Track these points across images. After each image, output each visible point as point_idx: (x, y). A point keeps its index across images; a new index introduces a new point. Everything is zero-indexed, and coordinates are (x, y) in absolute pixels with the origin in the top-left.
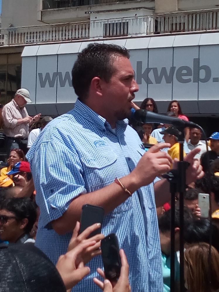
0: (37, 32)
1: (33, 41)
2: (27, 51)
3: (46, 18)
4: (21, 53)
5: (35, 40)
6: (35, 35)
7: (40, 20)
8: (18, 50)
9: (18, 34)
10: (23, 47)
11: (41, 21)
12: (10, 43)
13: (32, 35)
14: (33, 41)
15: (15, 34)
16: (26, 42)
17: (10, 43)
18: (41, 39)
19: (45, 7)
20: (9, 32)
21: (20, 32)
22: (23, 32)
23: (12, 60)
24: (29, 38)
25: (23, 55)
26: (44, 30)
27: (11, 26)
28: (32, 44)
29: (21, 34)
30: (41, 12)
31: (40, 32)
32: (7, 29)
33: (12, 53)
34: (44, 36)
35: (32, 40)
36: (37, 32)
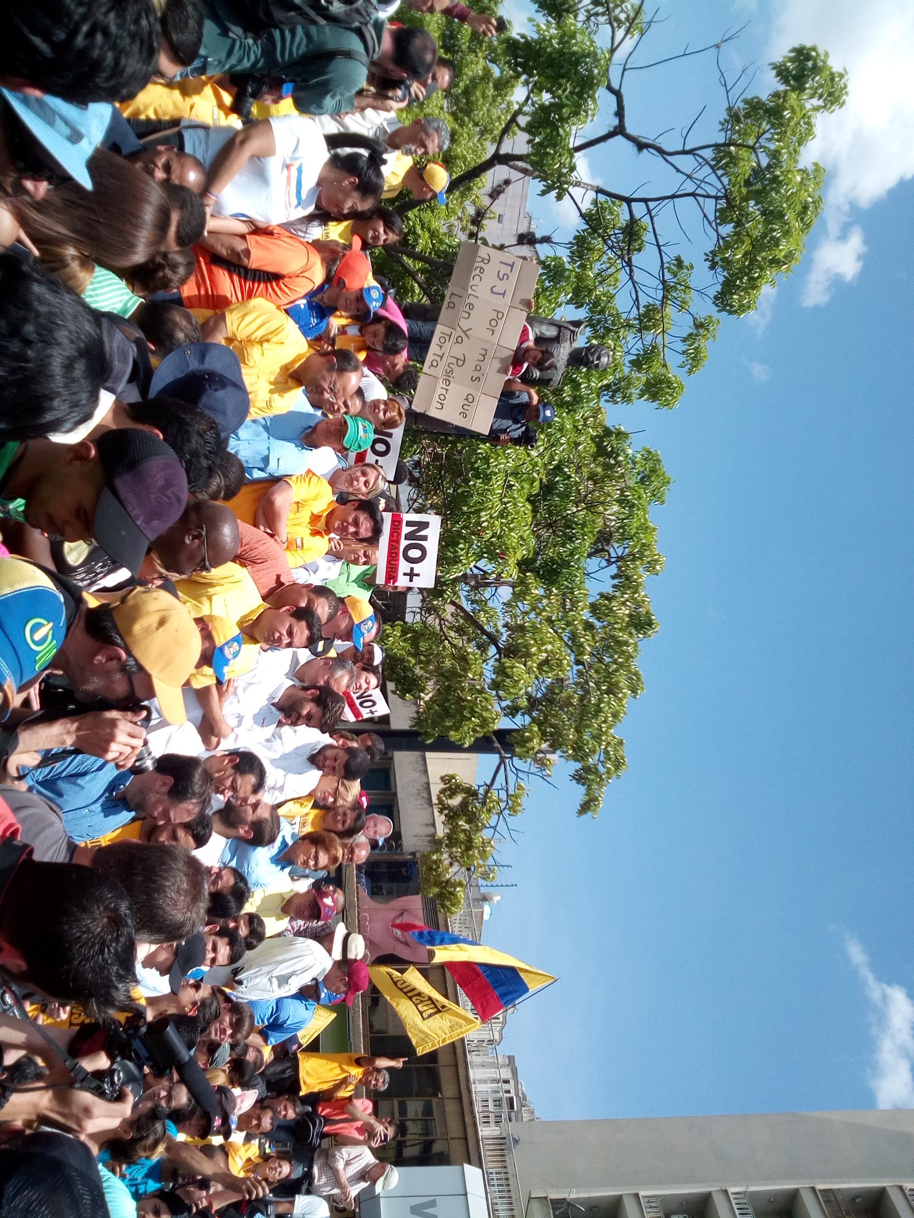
0: (509, 1191)
1: (494, 1185)
2: (473, 1174)
3: (535, 1205)
4: (470, 1163)
5: (496, 1188)
6: (505, 1188)
7: (532, 1196)
8: (474, 1157)
9: (503, 1155)
10: (481, 1167)
11: (530, 1198)
12: (486, 1142)
13: (503, 1182)
14: (494, 1185)
15: (503, 1150)
16: (490, 1170)
17: (486, 1142)
18: (498, 1201)
19: (556, 1203)
20: (504, 1138)
21: (507, 1159)
22: (508, 1164)
23: (456, 1148)
24: (499, 1176)
25: (467, 1167)
26: (515, 1206)
27: (516, 1141)
28: (487, 1182)
29: (503, 1155)
30: (546, 1198)
31: (510, 1197)
32: (508, 1134)
33: (468, 1150)
34: (505, 1207)
35: (495, 1182)
36: (509, 1191)
